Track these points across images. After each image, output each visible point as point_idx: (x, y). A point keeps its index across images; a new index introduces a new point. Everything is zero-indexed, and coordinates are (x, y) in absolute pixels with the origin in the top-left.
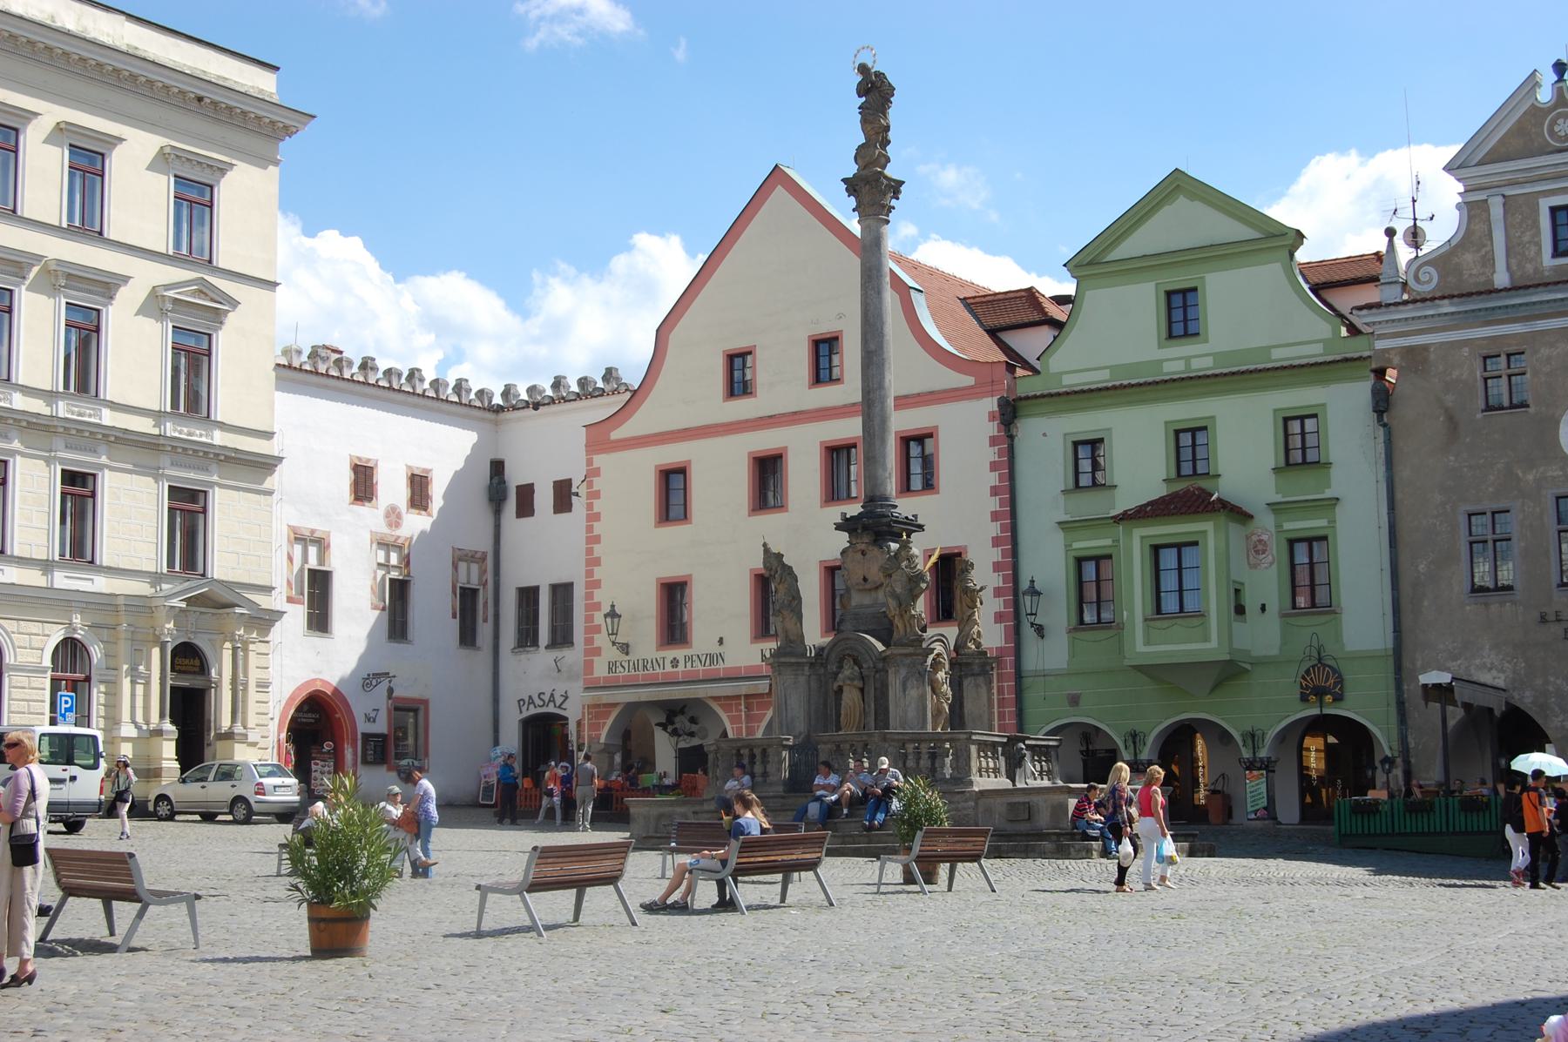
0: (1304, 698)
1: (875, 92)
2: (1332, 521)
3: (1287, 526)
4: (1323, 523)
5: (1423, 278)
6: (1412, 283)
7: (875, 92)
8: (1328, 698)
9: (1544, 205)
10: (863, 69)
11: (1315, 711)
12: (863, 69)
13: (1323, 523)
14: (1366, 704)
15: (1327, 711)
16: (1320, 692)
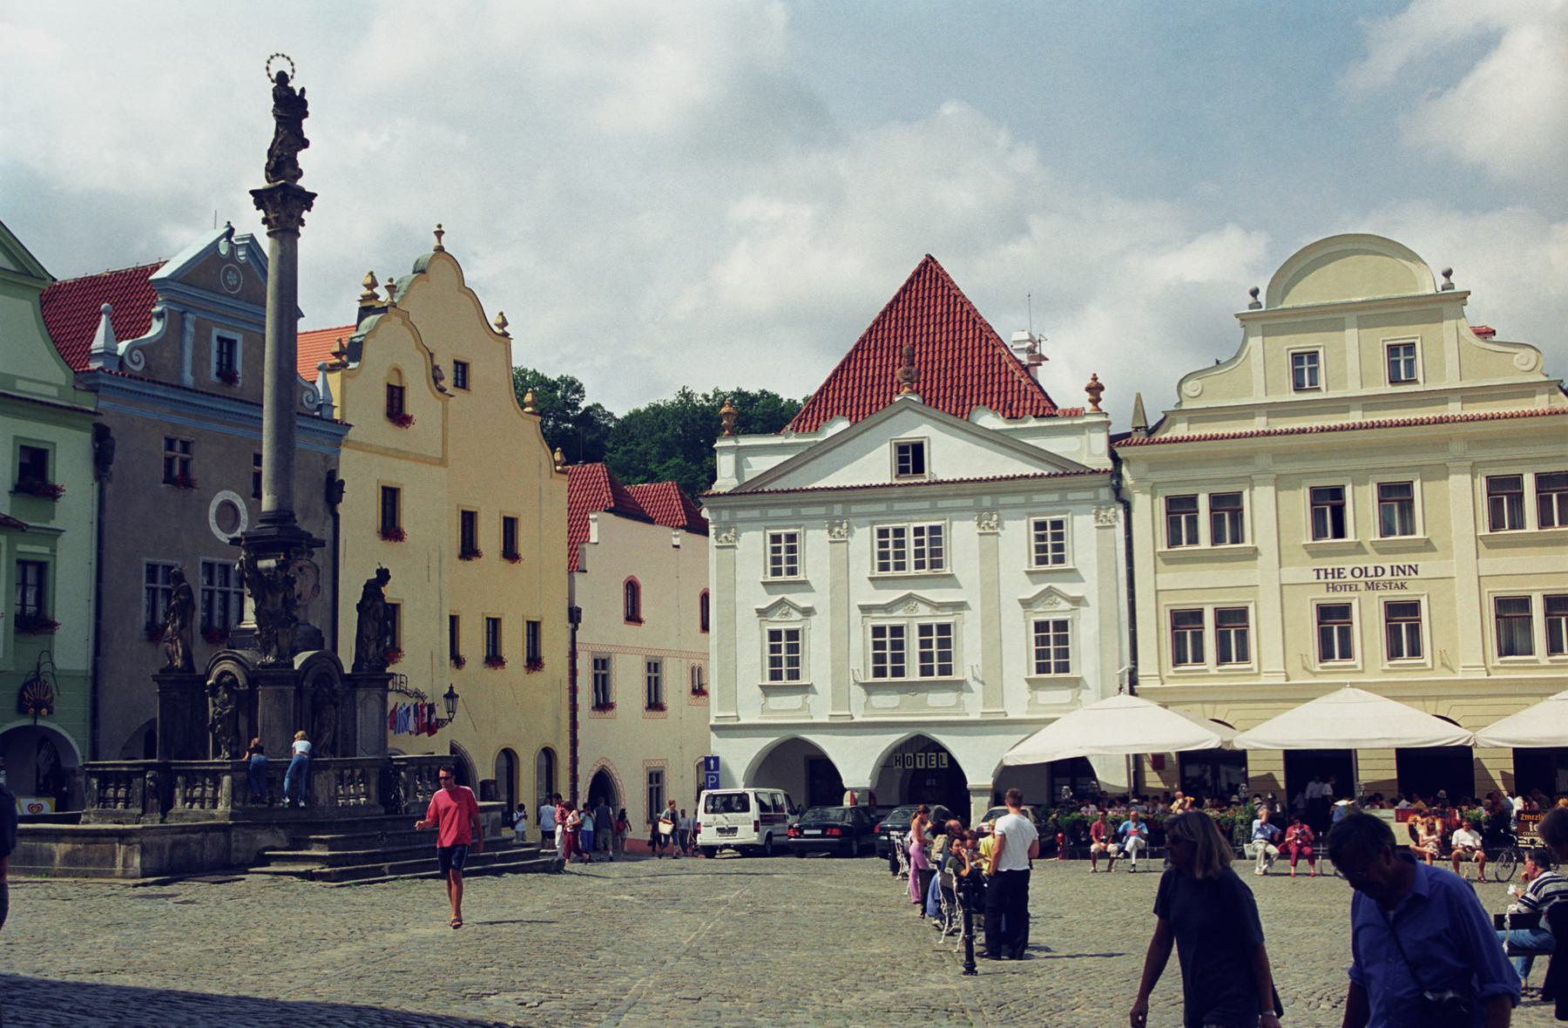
0: (22, 709)
1: (290, 107)
2: (54, 550)
3: (20, 548)
4: (46, 550)
5: (136, 359)
6: (127, 361)
7: (290, 107)
8: (44, 711)
9: (216, 332)
10: (282, 79)
11: (25, 722)
12: (282, 79)
13: (46, 550)
14: (66, 721)
15: (40, 723)
16: (39, 705)
